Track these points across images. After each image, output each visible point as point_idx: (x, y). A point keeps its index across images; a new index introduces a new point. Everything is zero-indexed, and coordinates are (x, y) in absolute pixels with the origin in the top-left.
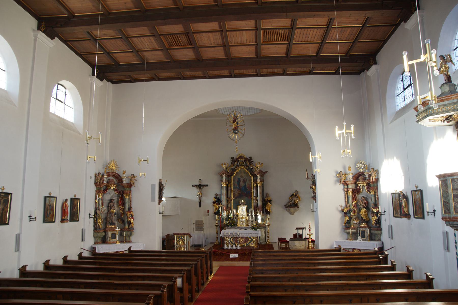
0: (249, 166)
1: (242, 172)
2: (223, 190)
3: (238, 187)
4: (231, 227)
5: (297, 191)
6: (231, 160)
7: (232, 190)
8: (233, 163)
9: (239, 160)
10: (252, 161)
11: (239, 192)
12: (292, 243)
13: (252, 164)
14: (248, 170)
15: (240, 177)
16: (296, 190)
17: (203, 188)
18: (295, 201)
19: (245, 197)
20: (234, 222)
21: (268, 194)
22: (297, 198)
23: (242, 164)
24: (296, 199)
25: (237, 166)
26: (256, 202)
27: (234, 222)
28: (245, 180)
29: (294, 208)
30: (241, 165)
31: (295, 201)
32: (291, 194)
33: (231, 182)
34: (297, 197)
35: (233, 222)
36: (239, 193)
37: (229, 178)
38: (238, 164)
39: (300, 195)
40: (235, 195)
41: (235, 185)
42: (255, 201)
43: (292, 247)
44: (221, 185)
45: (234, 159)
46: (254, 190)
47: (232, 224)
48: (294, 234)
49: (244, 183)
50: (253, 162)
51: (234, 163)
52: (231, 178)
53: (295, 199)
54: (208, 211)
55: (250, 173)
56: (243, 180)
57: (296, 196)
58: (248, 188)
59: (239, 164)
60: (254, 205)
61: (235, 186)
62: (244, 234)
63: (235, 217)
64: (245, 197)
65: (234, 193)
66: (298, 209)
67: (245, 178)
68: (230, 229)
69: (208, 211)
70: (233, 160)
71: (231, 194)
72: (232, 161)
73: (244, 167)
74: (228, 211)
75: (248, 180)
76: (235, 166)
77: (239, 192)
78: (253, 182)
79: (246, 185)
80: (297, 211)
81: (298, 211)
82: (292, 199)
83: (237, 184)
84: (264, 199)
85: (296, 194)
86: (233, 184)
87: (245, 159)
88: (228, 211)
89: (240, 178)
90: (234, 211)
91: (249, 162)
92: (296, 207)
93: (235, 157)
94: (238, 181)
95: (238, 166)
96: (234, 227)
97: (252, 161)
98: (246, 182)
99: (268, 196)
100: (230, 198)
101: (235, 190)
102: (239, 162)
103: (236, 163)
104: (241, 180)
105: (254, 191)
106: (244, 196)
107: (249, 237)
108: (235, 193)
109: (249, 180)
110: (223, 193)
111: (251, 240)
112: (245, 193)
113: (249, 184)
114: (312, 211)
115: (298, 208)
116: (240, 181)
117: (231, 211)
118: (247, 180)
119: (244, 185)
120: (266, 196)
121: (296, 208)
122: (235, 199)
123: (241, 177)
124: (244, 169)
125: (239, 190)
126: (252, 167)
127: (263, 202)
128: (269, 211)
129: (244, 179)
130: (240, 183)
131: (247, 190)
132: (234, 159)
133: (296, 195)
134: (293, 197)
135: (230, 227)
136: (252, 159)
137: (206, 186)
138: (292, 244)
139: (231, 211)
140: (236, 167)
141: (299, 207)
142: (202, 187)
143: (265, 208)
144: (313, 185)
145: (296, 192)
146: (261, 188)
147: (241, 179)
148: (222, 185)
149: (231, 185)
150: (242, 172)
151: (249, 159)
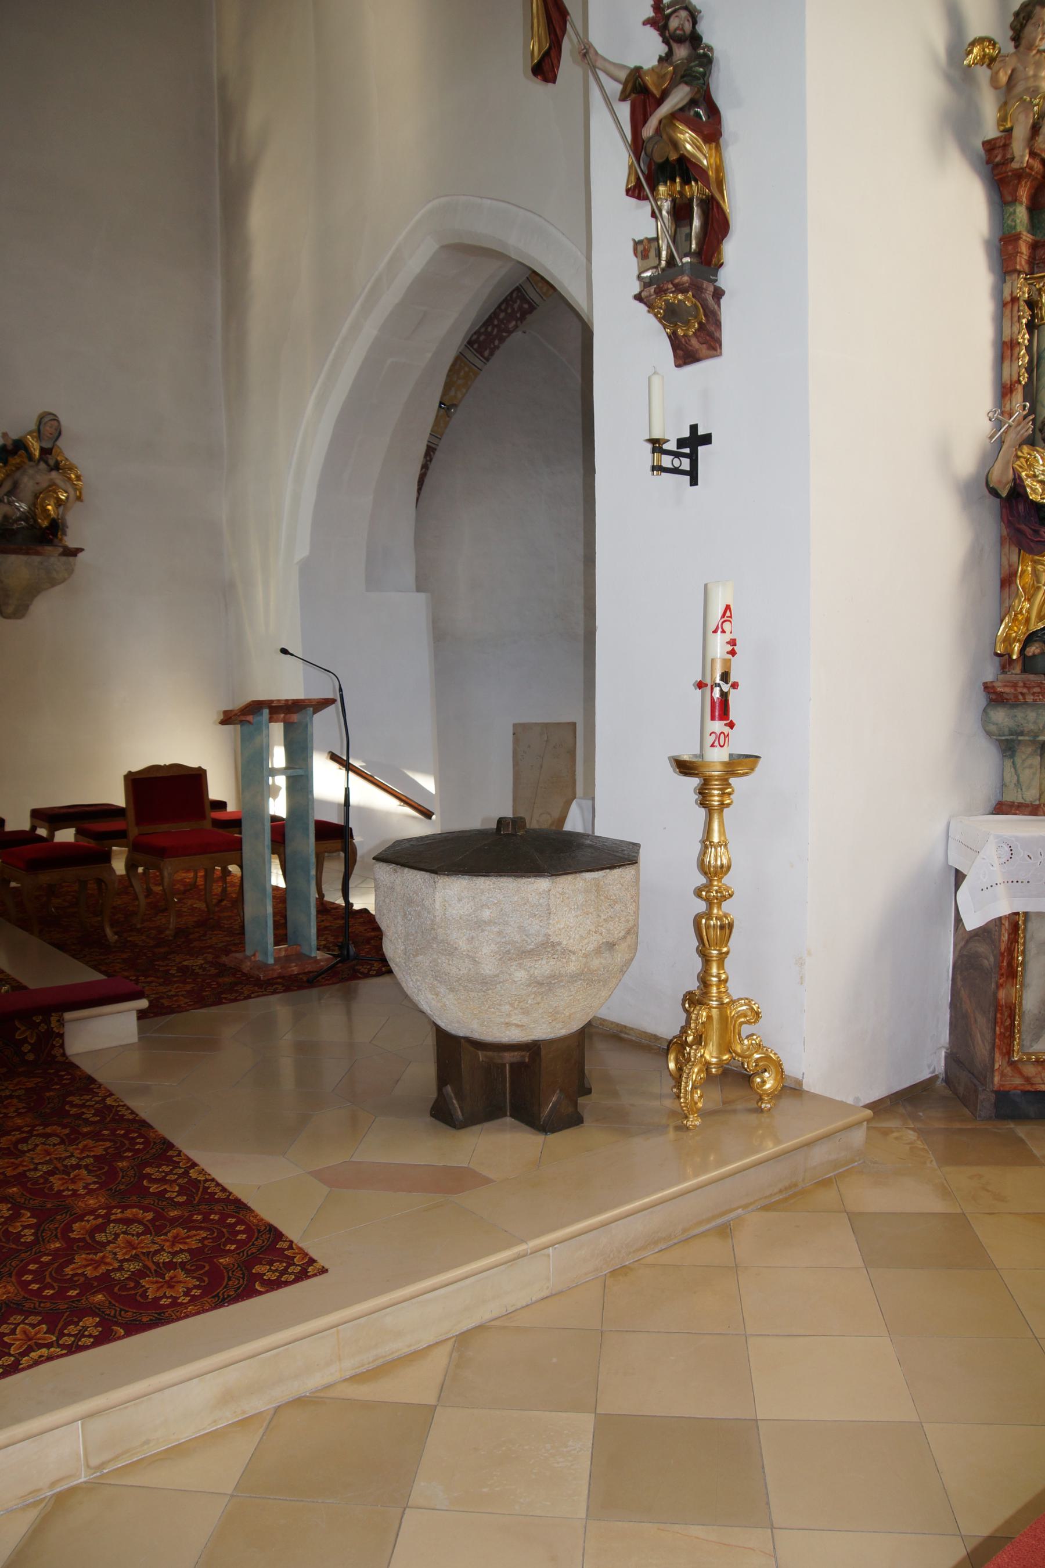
5: (55, 419)
12: (486, 914)
16: (41, 411)
18: (36, 497)
22: (54, 474)
24: (52, 488)
29: (37, 559)
31: (36, 497)
32: (5, 435)
34: (57, 467)
39: (69, 450)
43: (488, 968)
48: (137, 766)
53: (44, 485)
57: (52, 462)
66: (71, 571)
80: (53, 583)
81: (64, 580)
82: (15, 485)
85: (47, 445)
92: (49, 548)
114: (657, 468)
115: (71, 559)
121: (54, 559)
133: (45, 452)
134: (19, 467)
138: (480, 925)
141: (74, 552)
144: (694, 125)
145: (47, 429)
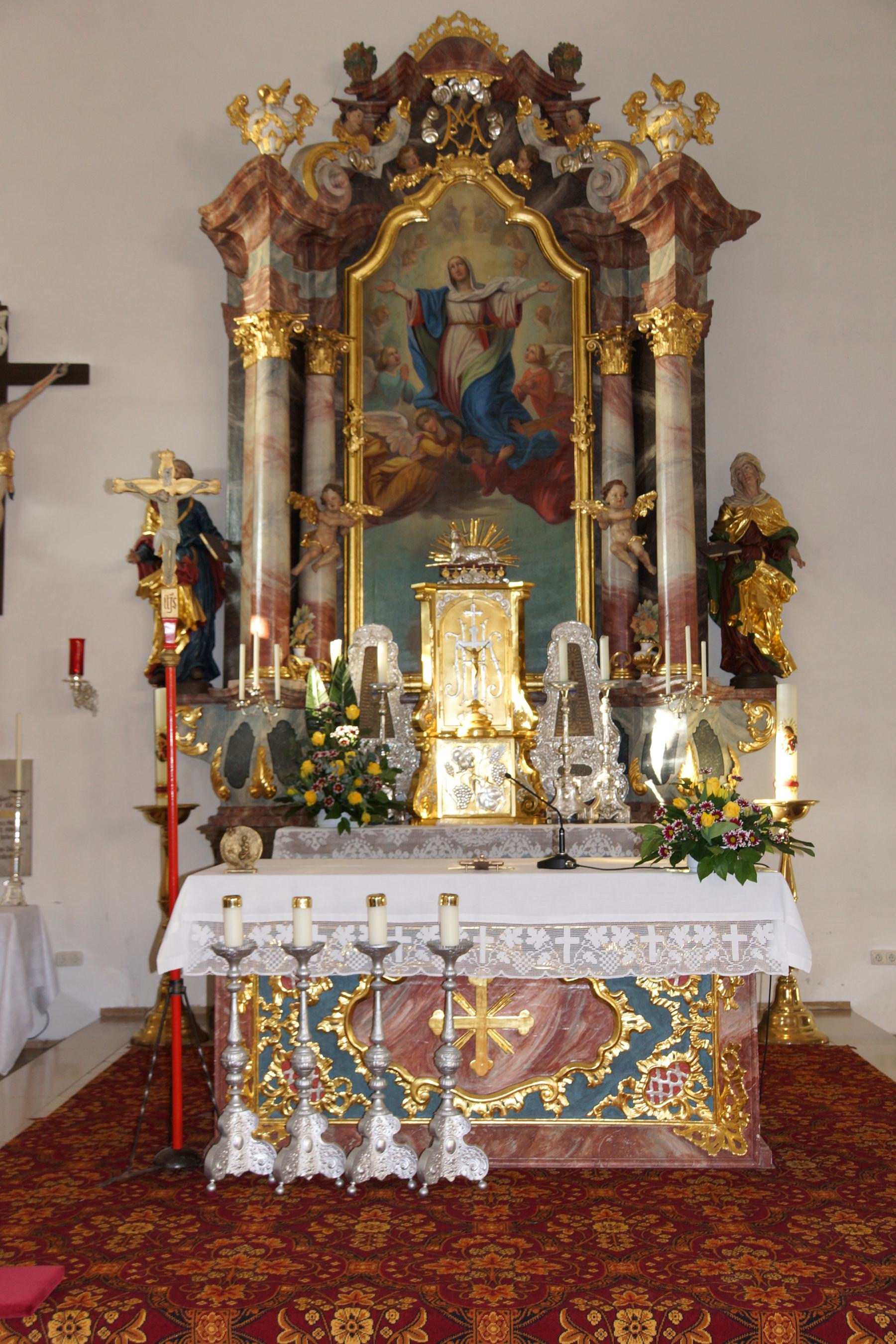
0: (552, 155)
1: (469, 217)
2: (248, 412)
3: (417, 384)
4: (344, 826)
6: (348, 81)
7: (356, 416)
8: (372, 118)
9: (438, 80)
10: (576, 96)
11: (429, 445)
13: (586, 116)
14: (529, 199)
15: (447, 282)
17: (27, 398)
19: (497, 494)
20: (374, 769)
21: (757, 469)
23: (464, 134)
25: (411, 154)
26: (629, 550)
27: (374, 769)
28: (502, 308)
30: (451, 148)
33: (343, 327)
35: (364, 770)
36: (427, 460)
37: (321, 276)
38: (416, 133)
40: (387, 478)
41: (382, 367)
42: (612, 537)
44: (225, 363)
45: (375, 77)
46: (596, 418)
47: (356, 798)
49: (485, 347)
50: (588, 103)
51: (383, 117)
52: (343, 282)
54: (77, 648)
55: (561, 236)
56: (476, 307)
58: (528, 404)
59: (430, 138)
60: (598, 590)
61: (390, 378)
62: (538, 938)
63: (389, 718)
64: (497, 494)
65: (374, 449)
67: (499, 291)
68: (325, 850)
69: (77, 648)
70: (368, 82)
71: (340, 468)
72: (353, 98)
73: (495, 167)
74: (300, 650)
75: (526, 308)
76: (383, 155)
77: (429, 445)
78: (593, 326)
79: (505, 367)
83: (407, 357)
84: (710, 525)
86: (370, 351)
87: (498, 66)
88: (300, 650)
89: (446, 291)
90: (371, 653)
91: (545, 114)
93: (385, 63)
94: (419, 326)
95: (427, 154)
96: (370, 831)
97: (576, 96)
98: (508, 341)
99: (752, 482)
100: (331, 494)
101: (388, 420)
102: (432, 115)
103: (399, 114)
104: (456, 311)
105: (596, 439)
106: (489, 492)
107: (612, 985)
108: (386, 454)
109: (545, 317)
110: (247, 447)
111: (641, 1023)
112: (504, 453)
113: (542, 359)
116: (447, 323)
117: (336, 647)
118: (519, 307)
119: (487, 368)
120: (731, 493)
122: (396, 512)
123: (454, 282)
124: (491, 185)
125: (431, 423)
126: (578, 154)
127: (702, 550)
128: (765, 651)
129: (485, 302)
130: (440, 341)
131: (524, 418)
132: (375, 77)
135: (327, 825)
136: (578, 77)
137: (58, 382)
139: (336, 647)
140: (396, 166)
142: (15, 393)
143: (721, 620)
146: (685, 392)
147: (453, 295)
148: (236, 353)
149: (342, 359)
150: (469, 217)
151: (547, 69)
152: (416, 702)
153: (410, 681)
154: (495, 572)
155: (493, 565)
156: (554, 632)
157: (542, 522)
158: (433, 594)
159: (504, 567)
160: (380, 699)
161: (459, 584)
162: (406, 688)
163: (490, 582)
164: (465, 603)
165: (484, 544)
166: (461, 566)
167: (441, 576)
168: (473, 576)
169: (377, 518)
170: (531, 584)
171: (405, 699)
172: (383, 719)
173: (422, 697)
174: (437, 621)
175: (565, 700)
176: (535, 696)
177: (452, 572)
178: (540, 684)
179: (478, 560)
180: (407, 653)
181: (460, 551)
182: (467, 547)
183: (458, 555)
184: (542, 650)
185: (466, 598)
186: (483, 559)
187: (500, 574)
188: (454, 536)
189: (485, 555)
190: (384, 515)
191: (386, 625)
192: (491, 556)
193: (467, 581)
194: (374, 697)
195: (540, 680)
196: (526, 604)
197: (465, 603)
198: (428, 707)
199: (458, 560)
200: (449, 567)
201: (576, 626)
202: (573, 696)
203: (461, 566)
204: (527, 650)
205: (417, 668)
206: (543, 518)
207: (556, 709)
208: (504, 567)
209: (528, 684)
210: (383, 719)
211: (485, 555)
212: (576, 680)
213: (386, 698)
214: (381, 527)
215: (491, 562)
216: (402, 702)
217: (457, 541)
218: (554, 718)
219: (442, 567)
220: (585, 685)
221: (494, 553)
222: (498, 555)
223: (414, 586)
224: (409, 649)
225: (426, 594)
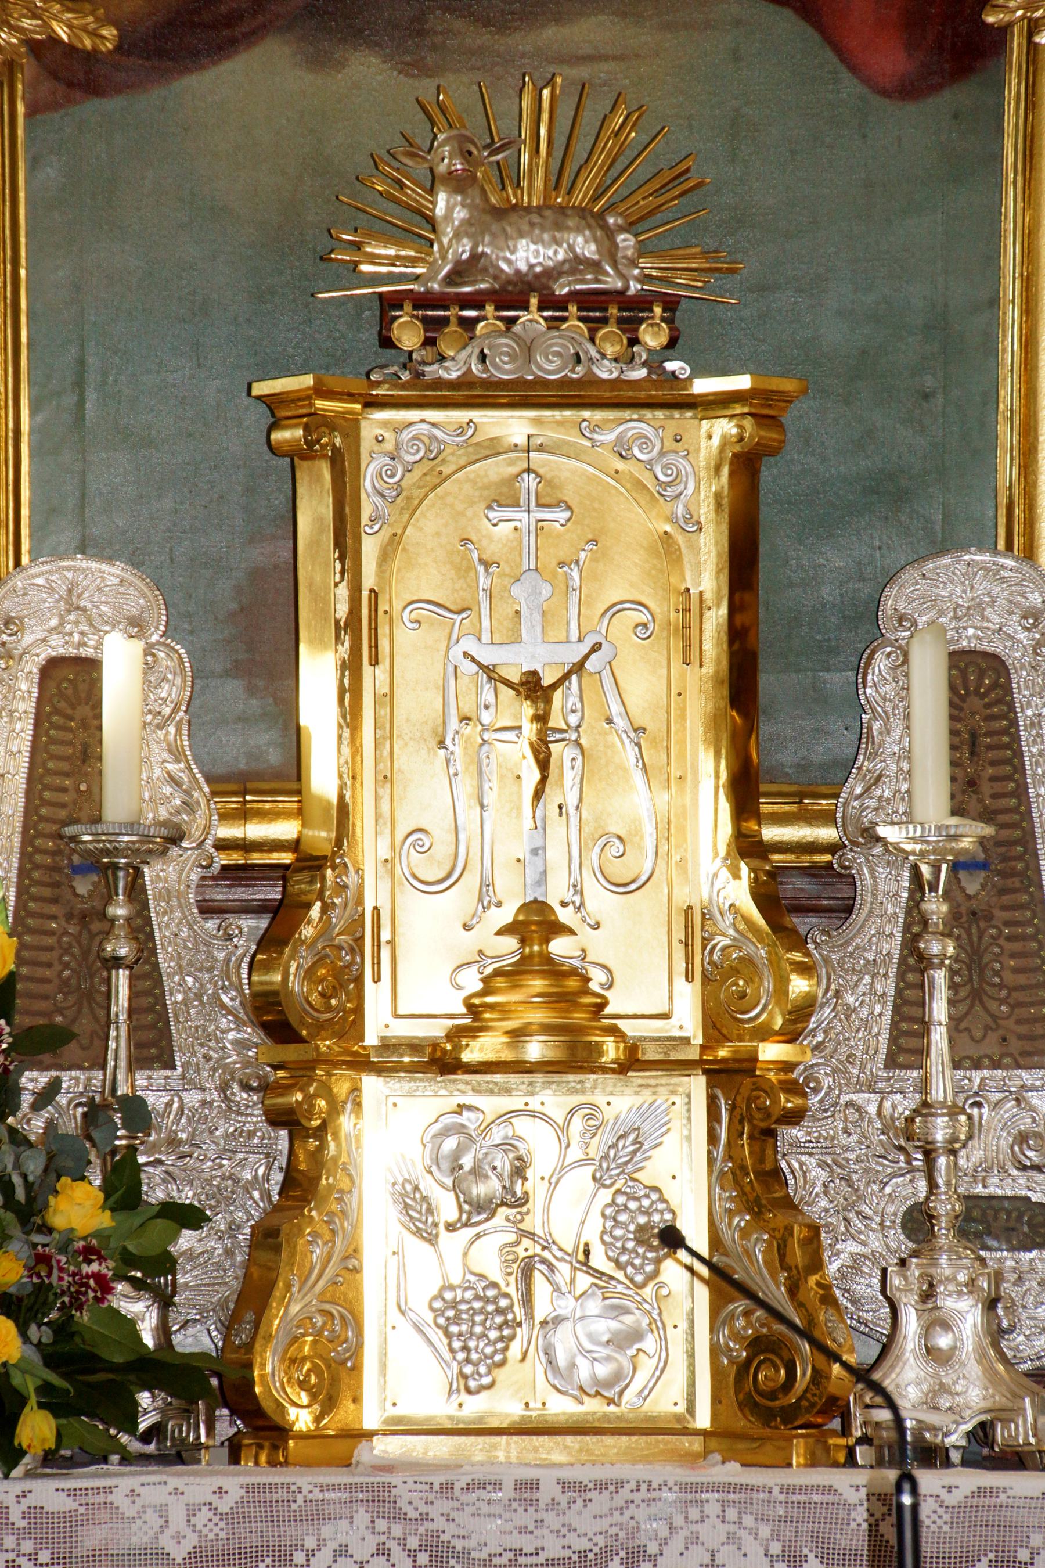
152: (273, 909)
153: (244, 815)
154: (630, 327)
155: (619, 296)
156: (893, 601)
157: (850, 86)
158: (351, 428)
159: (671, 304)
160: (109, 898)
161: (466, 382)
162: (222, 846)
163: (605, 372)
164: (496, 469)
165: (579, 197)
166: (475, 301)
167: (386, 342)
168: (528, 349)
169: (91, 57)
170: (789, 385)
171: (220, 894)
172: (122, 979)
173: (299, 885)
174: (370, 548)
175: (936, 907)
176: (799, 886)
177: (433, 326)
178: (827, 834)
179: (552, 274)
180: (233, 688)
181: (469, 229)
182: (500, 213)
183: (464, 249)
184: (836, 680)
185: (494, 448)
186: (577, 264)
187: (653, 337)
188: (449, 162)
189: (586, 247)
190: (119, 48)
191: (135, 562)
192: (611, 252)
193: (504, 369)
194: (83, 886)
195: (828, 818)
196: (767, 474)
197: (496, 469)
198: (325, 928)
199: (460, 272)
200: (423, 301)
201: (992, 572)
202: (972, 884)
203: (475, 301)
204: (768, 682)
205: (274, 757)
206: (853, 69)
207: (894, 947)
208: (671, 304)
209: (770, 833)
210: (122, 979)
211: (586, 247)
212: (986, 816)
213: (136, 891)
214: (113, 104)
215: (612, 282)
216: (207, 909)
217: (458, 183)
218: (887, 987)
219: (389, 303)
220: (1028, 840)
221: (626, 241)
222: (642, 250)
223: (261, 388)
224: (237, 670)
225: (315, 424)
